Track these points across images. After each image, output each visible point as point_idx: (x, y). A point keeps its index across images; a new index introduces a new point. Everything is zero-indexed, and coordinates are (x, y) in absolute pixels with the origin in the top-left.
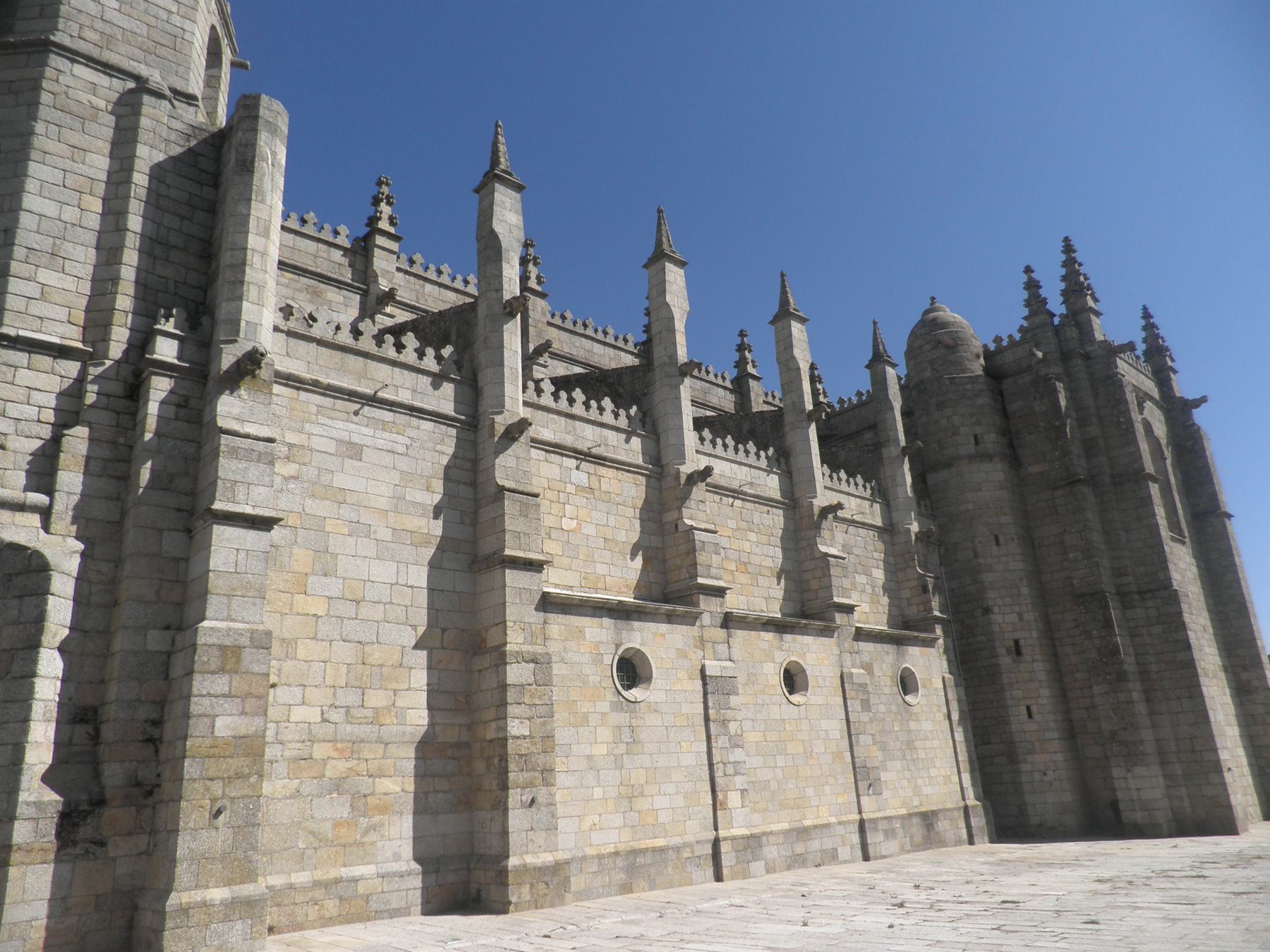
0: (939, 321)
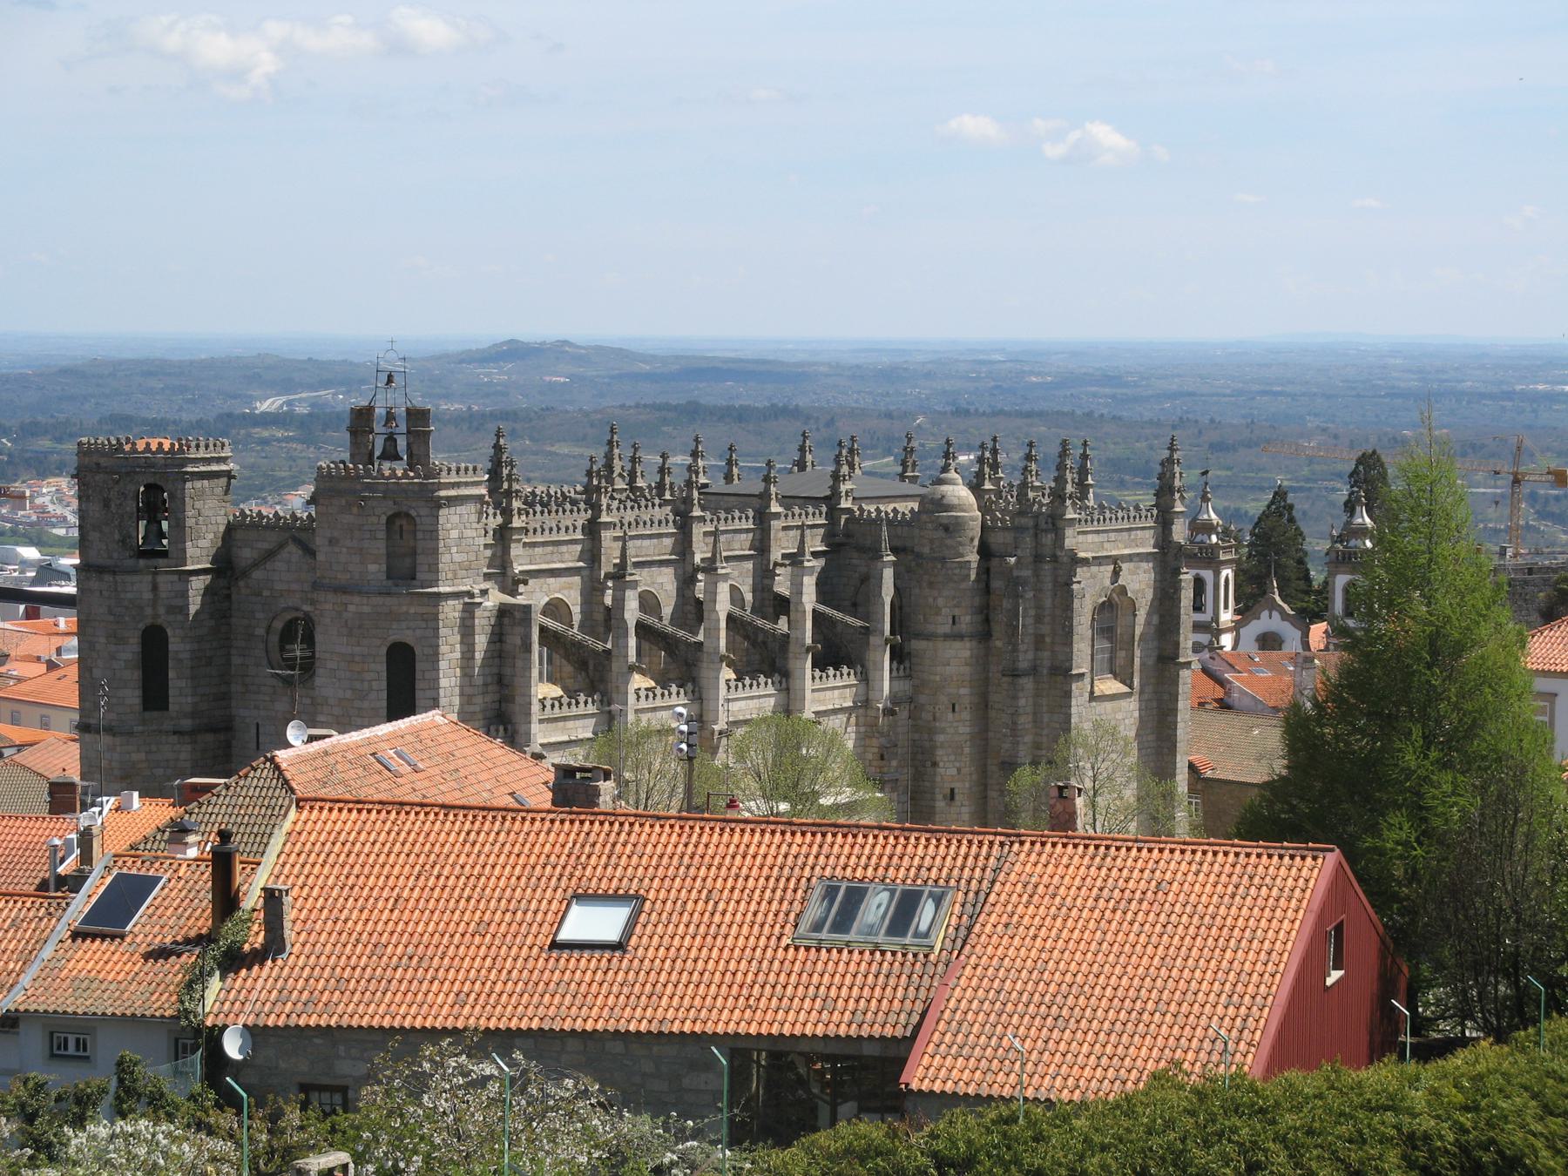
0: (945, 501)
